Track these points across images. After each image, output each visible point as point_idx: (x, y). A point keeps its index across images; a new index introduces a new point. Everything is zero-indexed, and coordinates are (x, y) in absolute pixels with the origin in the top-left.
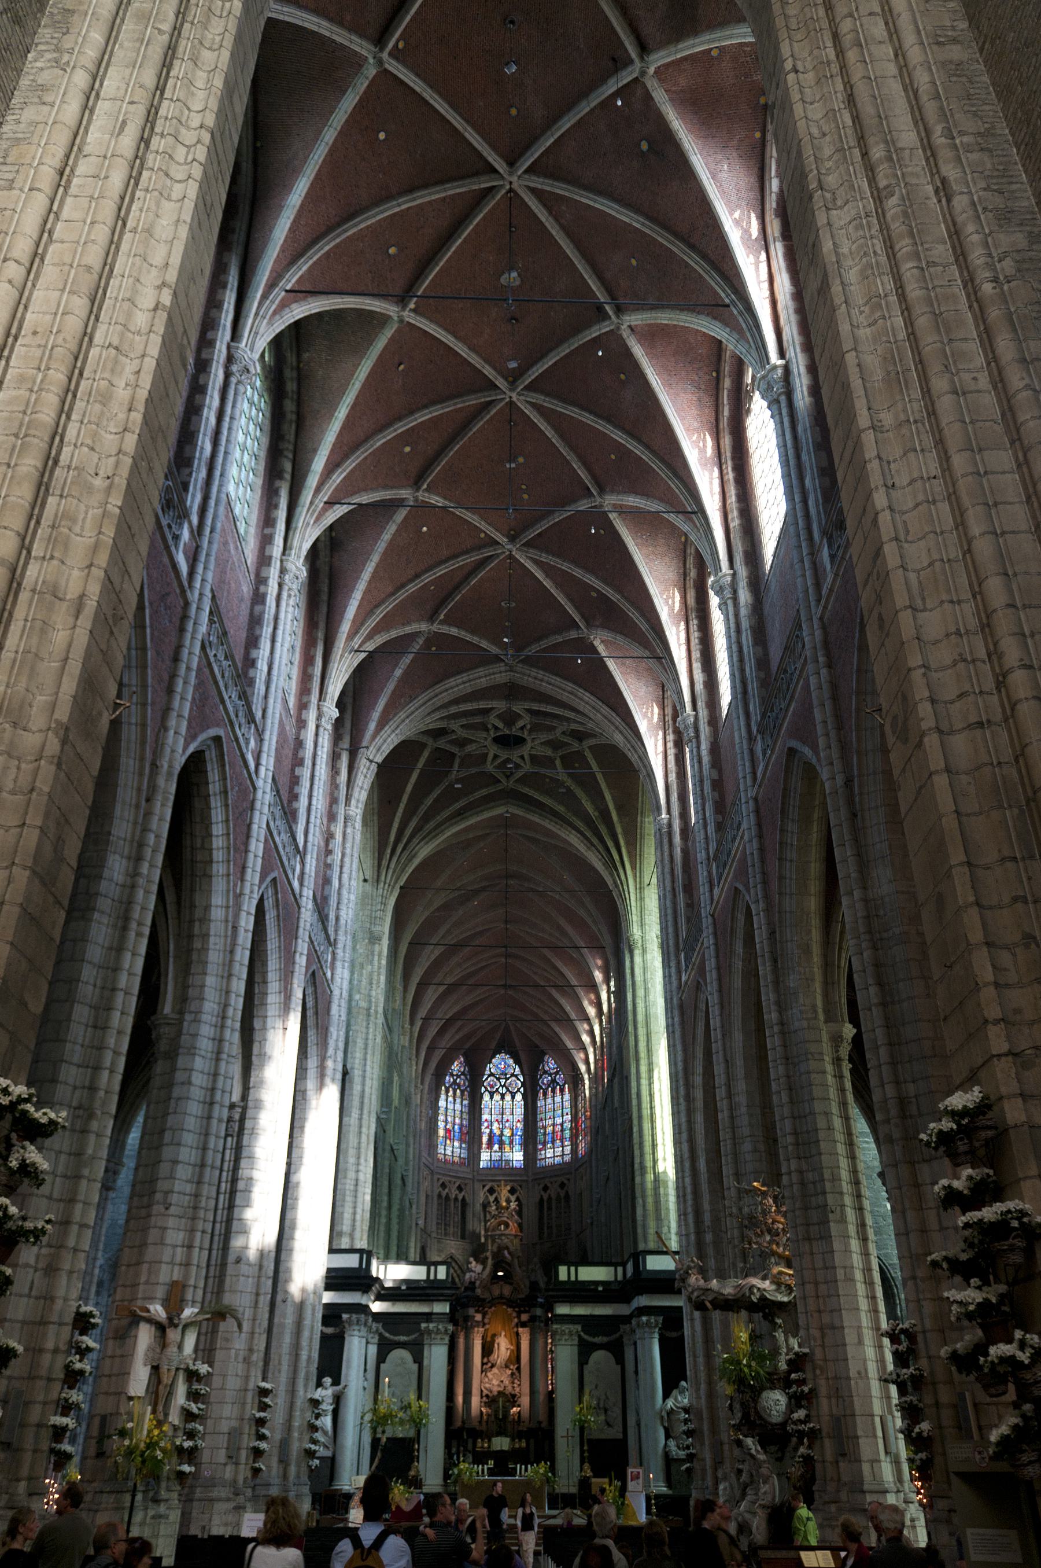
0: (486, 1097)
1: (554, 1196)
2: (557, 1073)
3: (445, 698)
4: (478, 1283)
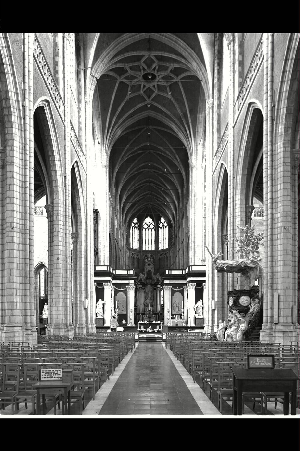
0: (144, 230)
1: (163, 257)
2: (164, 223)
3: (122, 46)
4: (143, 279)
